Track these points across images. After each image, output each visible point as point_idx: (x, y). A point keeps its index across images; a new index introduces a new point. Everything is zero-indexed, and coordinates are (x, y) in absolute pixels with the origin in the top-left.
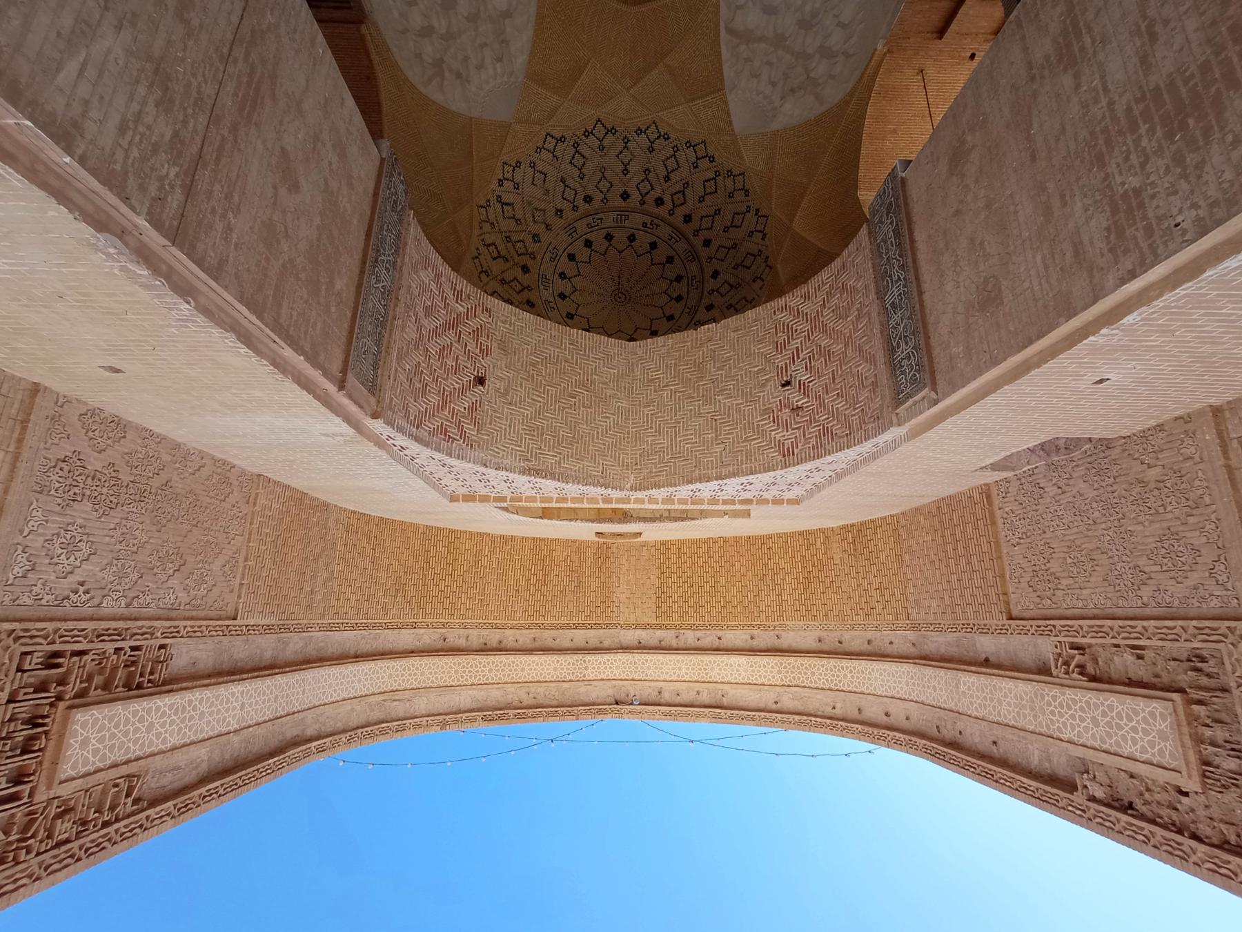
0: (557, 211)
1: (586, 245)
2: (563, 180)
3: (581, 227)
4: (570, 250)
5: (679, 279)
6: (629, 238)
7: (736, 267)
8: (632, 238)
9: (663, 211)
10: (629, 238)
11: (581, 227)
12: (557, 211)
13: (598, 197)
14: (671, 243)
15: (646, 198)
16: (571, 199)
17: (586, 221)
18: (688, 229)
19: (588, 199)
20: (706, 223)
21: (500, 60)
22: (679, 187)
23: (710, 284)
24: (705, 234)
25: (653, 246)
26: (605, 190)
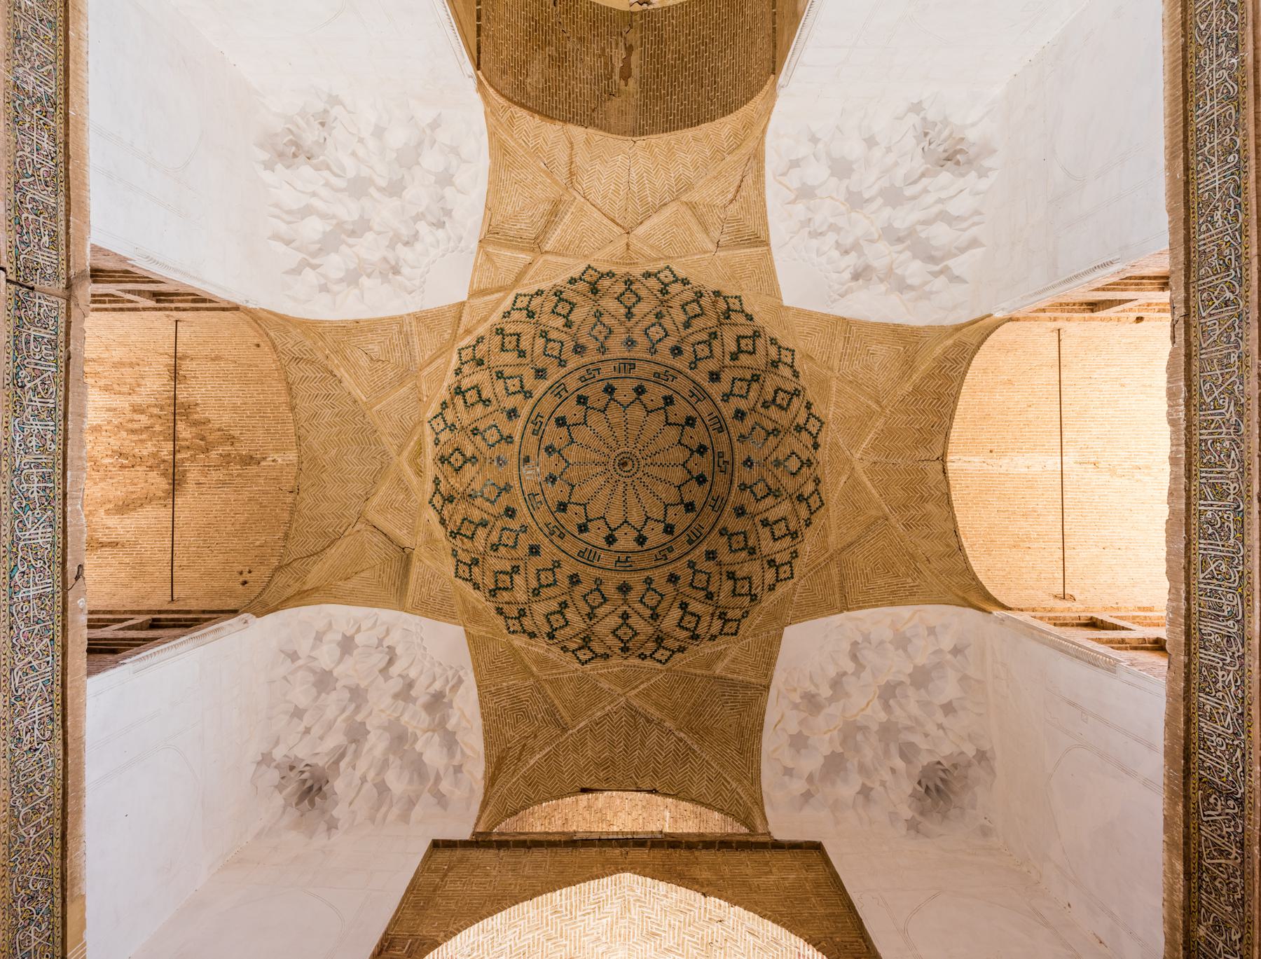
0: (538, 371)
1: (579, 402)
2: (544, 334)
3: (572, 383)
4: (558, 414)
5: (702, 450)
6: (636, 390)
7: (777, 463)
8: (640, 391)
9: (681, 364)
10: (636, 390)
11: (572, 383)
12: (538, 371)
13: (592, 345)
14: (693, 400)
15: (659, 347)
16: (556, 353)
17: (577, 375)
18: (716, 390)
19: (579, 349)
20: (740, 387)
21: (440, 225)
22: (705, 337)
23: (743, 475)
24: (736, 403)
25: (668, 401)
26: (601, 338)
